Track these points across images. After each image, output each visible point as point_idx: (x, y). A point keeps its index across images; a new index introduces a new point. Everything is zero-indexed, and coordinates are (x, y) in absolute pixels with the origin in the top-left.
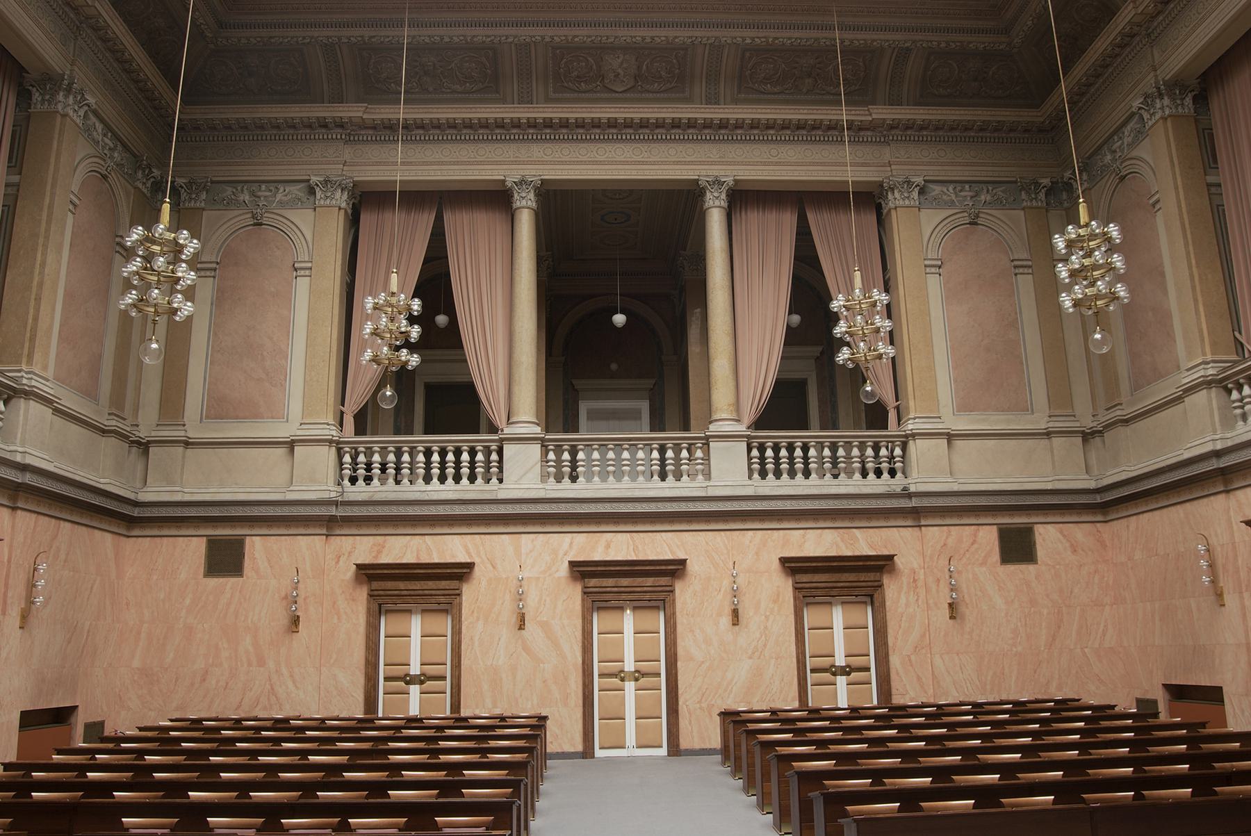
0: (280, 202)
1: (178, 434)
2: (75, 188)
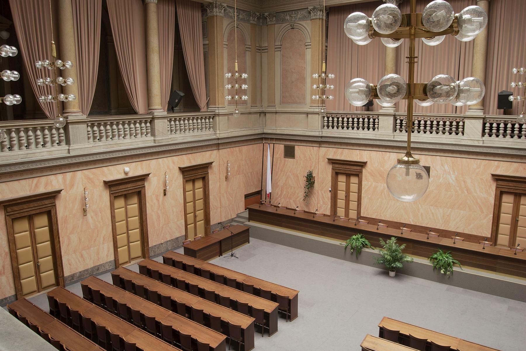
0: (299, 18)
1: (273, 110)
2: (225, 39)
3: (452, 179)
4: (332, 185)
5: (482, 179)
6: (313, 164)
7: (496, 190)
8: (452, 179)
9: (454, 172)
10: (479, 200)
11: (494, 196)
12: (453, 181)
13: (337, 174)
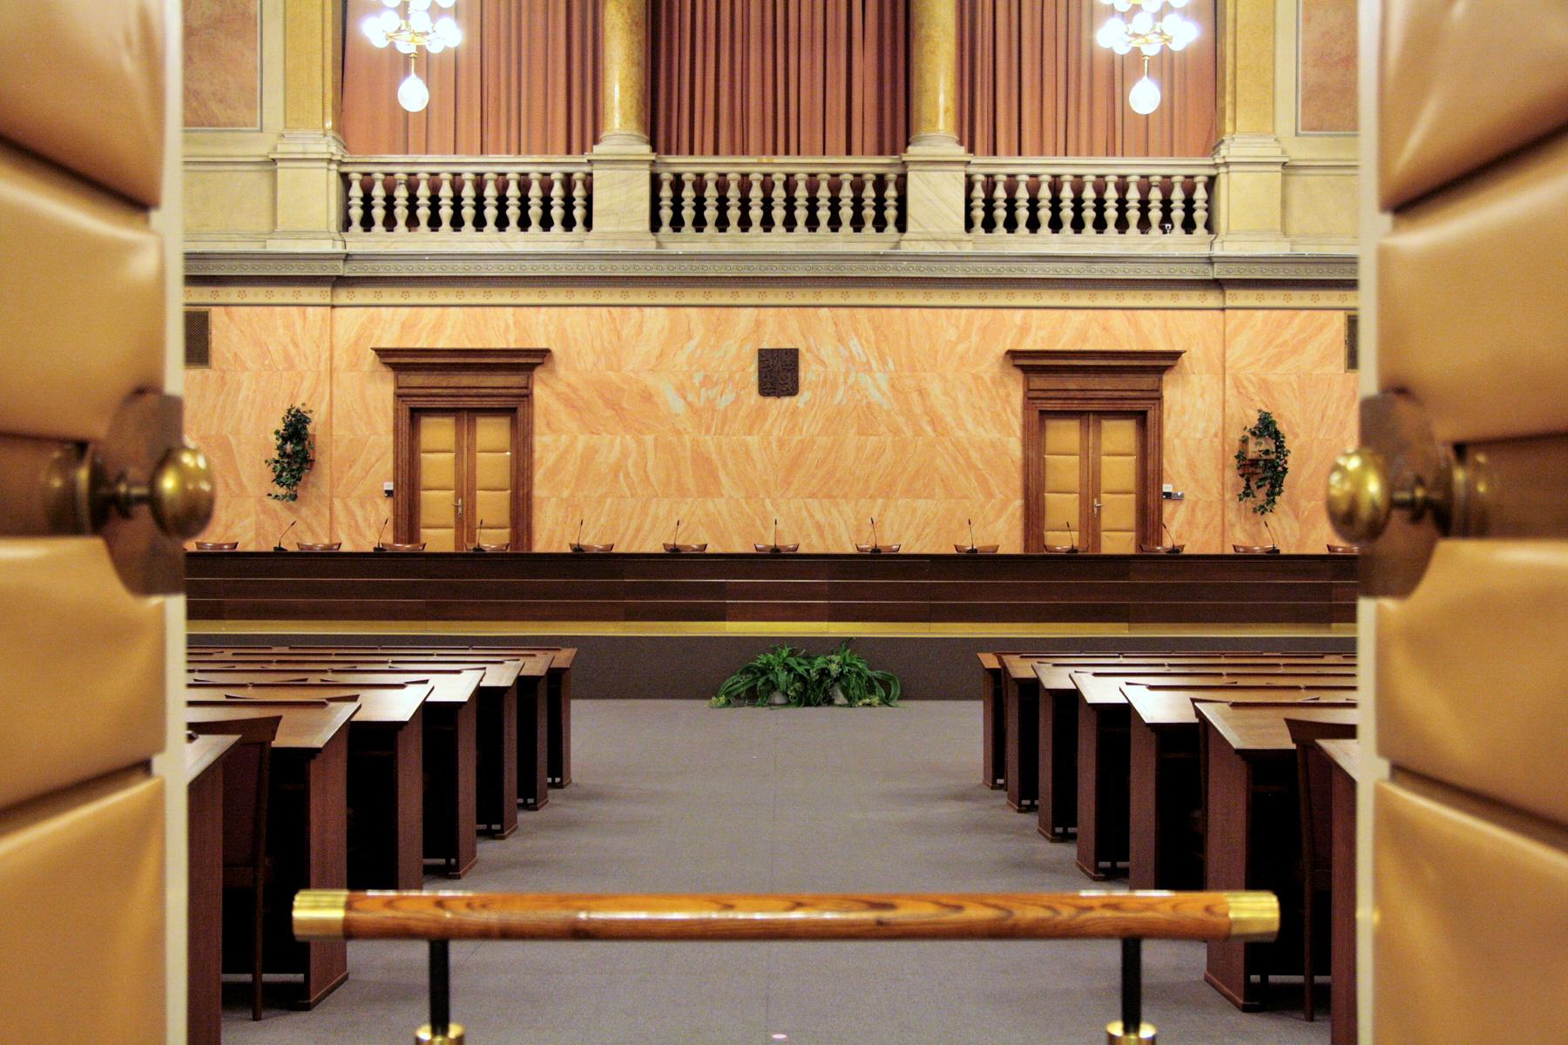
3: (878, 388)
4: (396, 468)
5: (976, 377)
6: (307, 384)
7: (1026, 408)
8: (876, 388)
9: (882, 360)
10: (974, 455)
11: (1019, 433)
12: (883, 394)
13: (416, 414)
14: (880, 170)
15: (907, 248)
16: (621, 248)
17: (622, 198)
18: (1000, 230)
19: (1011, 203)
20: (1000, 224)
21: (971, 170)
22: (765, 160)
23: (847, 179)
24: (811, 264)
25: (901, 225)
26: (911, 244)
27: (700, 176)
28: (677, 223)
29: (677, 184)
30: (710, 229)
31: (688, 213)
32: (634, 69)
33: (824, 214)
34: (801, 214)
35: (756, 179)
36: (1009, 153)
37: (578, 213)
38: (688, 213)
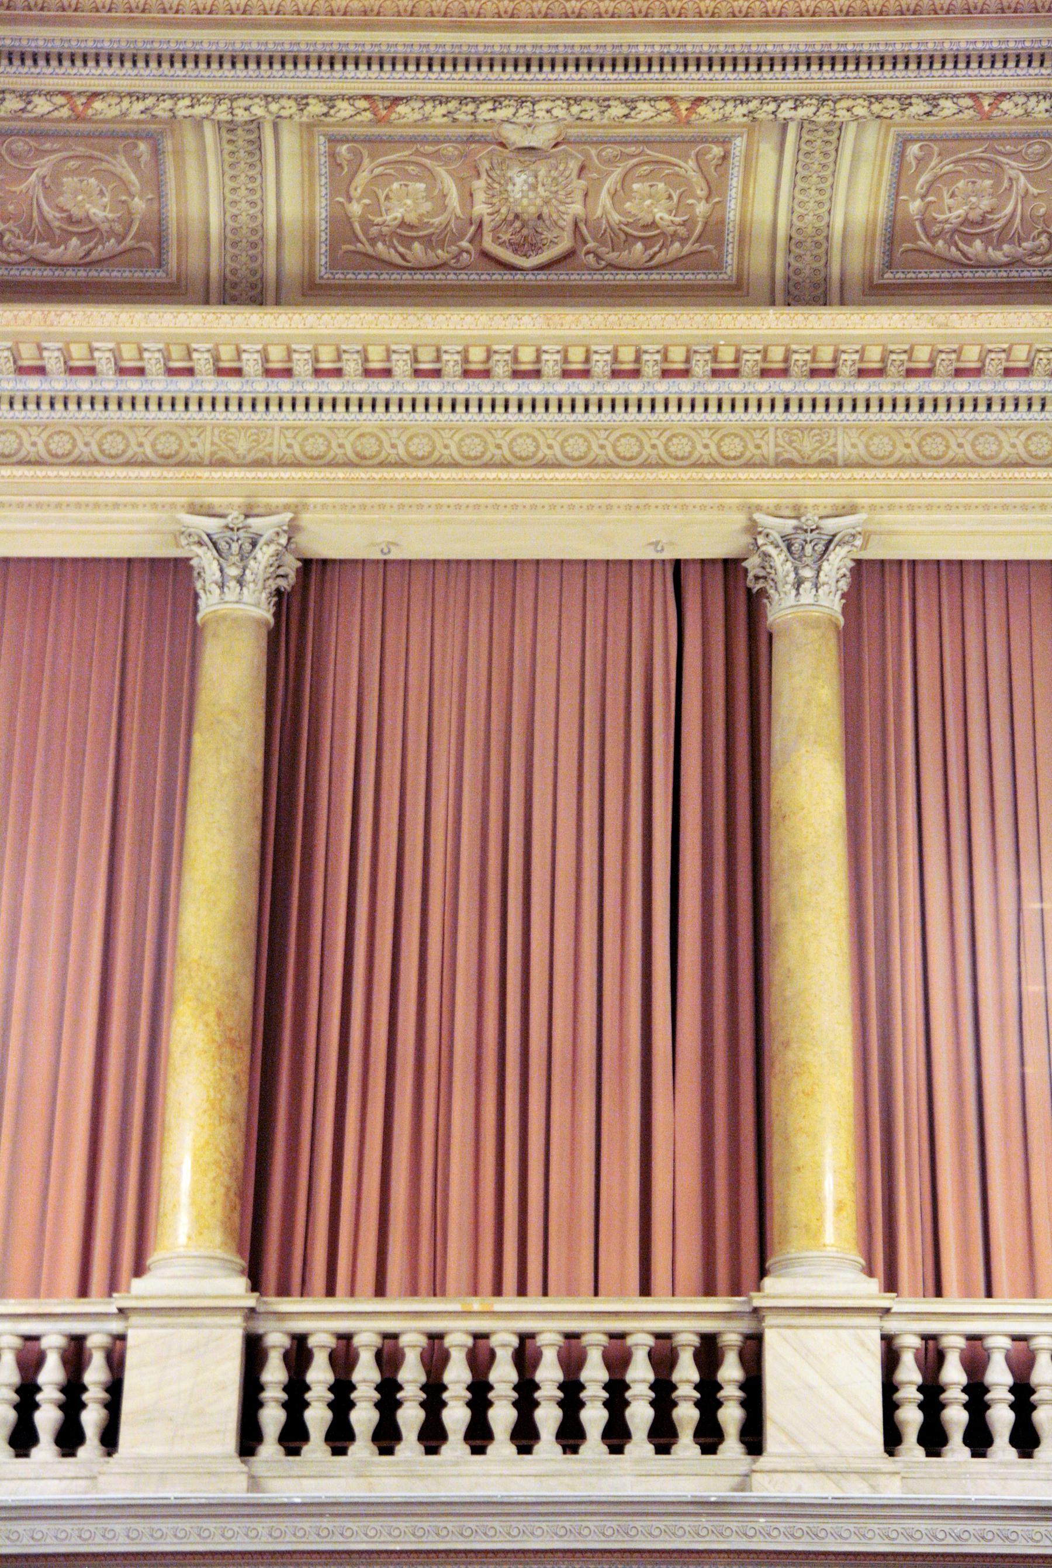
14: (708, 1326)
15: (767, 1487)
16: (172, 1492)
17: (182, 1386)
18: (957, 1450)
19: (977, 1396)
20: (956, 1437)
21: (892, 1325)
22: (476, 1304)
23: (641, 1344)
24: (567, 1523)
25: (753, 1439)
26: (775, 1478)
27: (345, 1338)
28: (294, 1437)
29: (299, 1355)
30: (362, 1448)
31: (317, 1416)
32: (224, 1129)
33: (594, 1416)
34: (548, 1417)
35: (457, 1344)
36: (967, 1293)
37: (92, 1418)
38: (317, 1416)
